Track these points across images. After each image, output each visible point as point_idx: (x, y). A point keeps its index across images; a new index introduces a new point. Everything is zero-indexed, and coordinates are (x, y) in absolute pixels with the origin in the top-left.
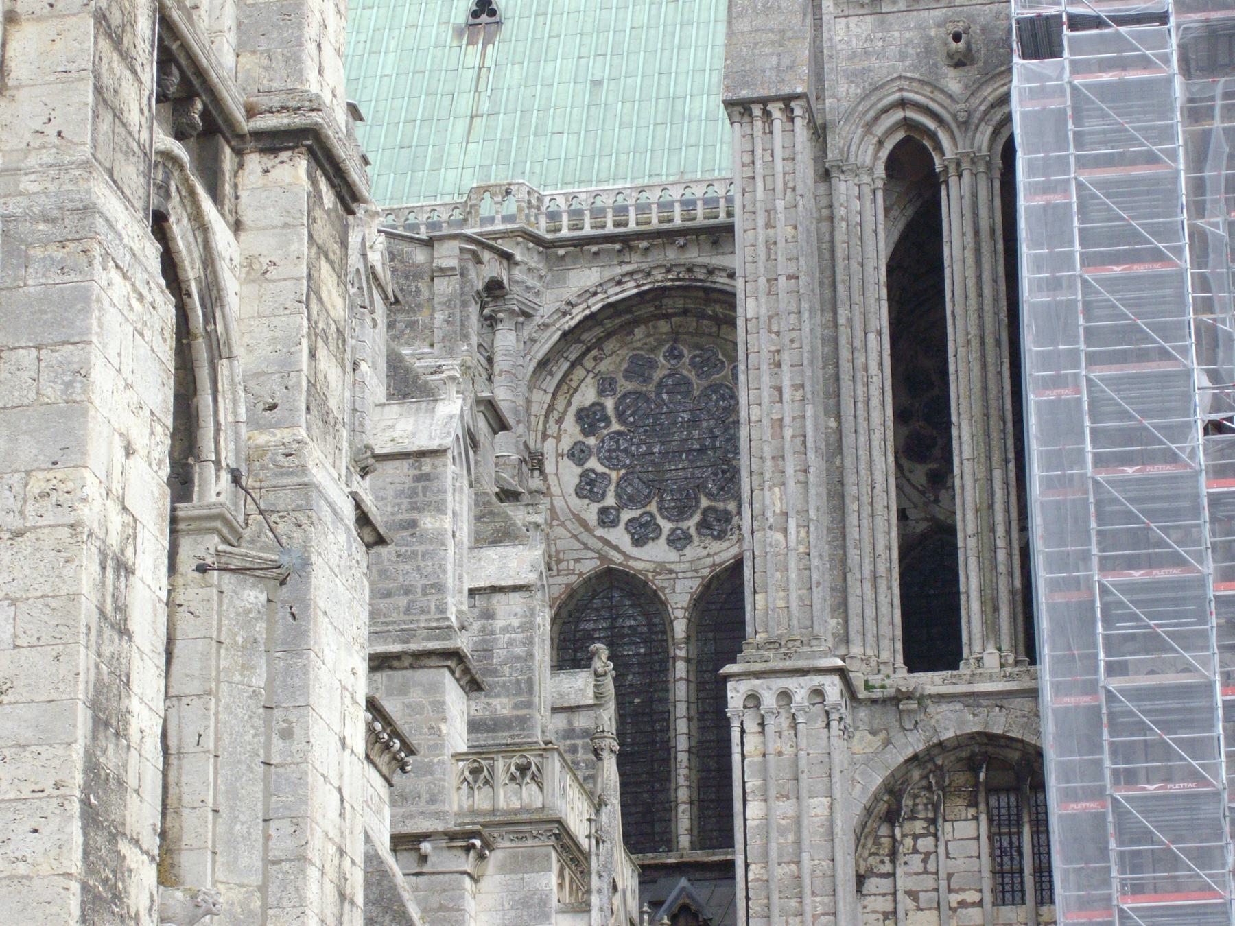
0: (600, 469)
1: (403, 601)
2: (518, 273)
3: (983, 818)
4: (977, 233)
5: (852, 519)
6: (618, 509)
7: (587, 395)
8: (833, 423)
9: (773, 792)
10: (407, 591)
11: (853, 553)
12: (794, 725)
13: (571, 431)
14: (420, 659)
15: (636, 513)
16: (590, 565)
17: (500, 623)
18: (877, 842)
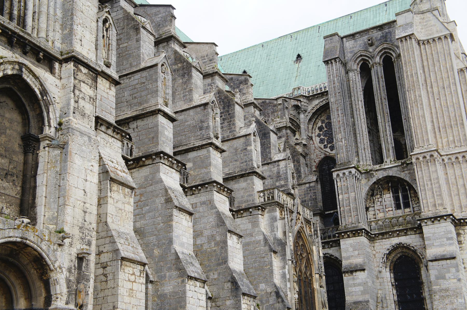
0: (323, 138)
1: (245, 164)
2: (302, 103)
3: (391, 193)
4: (378, 78)
5: (358, 138)
6: (327, 145)
7: (320, 124)
8: (353, 120)
9: (343, 193)
10: (246, 162)
11: (359, 145)
12: (346, 179)
13: (317, 131)
14: (249, 174)
15: (331, 145)
16: (323, 156)
17: (281, 167)
18: (370, 200)
